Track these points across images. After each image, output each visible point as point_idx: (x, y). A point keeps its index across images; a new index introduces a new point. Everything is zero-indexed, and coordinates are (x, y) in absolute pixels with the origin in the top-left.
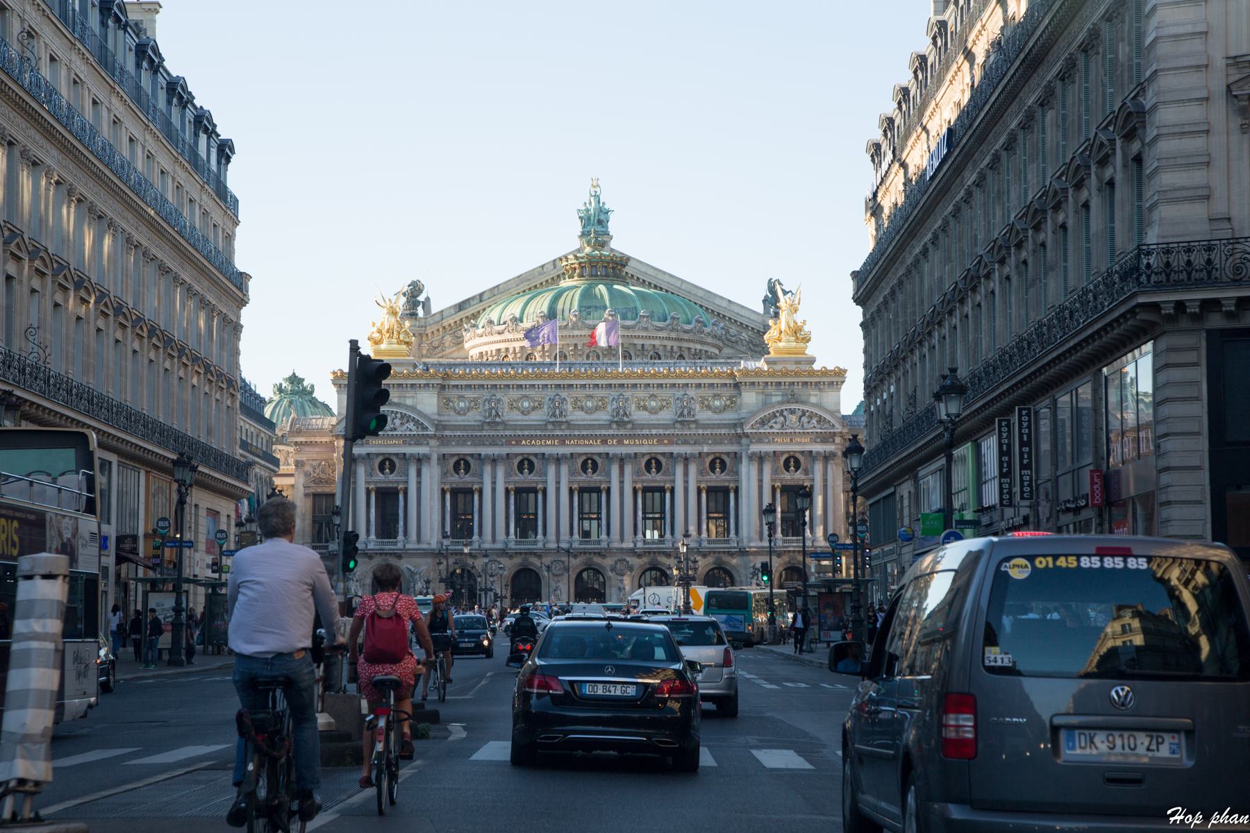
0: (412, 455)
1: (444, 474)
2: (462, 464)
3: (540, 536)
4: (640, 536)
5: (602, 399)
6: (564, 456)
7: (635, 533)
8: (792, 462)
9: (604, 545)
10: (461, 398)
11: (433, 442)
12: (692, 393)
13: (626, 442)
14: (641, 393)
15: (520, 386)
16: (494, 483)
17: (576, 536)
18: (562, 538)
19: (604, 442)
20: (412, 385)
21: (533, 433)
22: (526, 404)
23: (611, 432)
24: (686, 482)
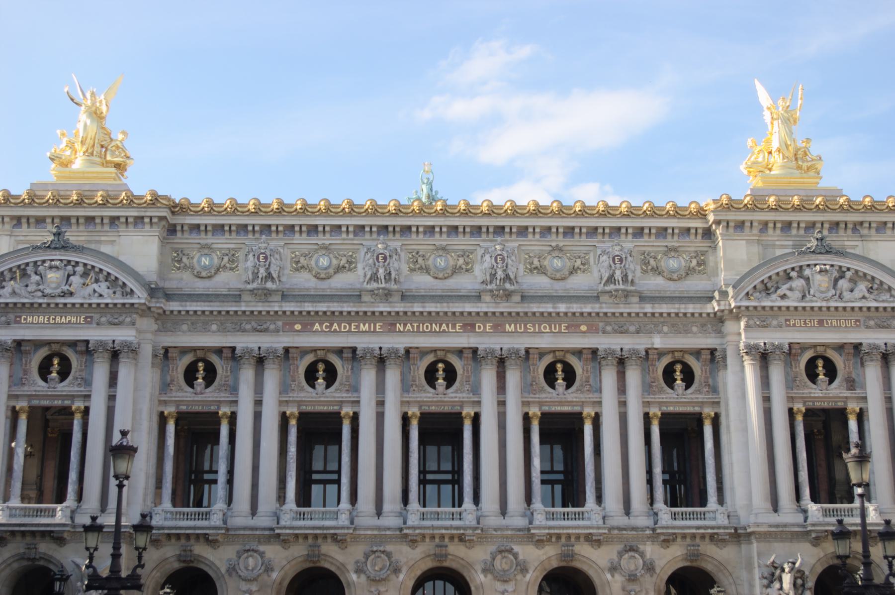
0: (101, 344)
1: (165, 386)
2: (201, 368)
3: (345, 504)
4: (537, 505)
5: (464, 254)
6: (394, 352)
7: (529, 499)
8: (821, 366)
9: (469, 519)
10: (206, 249)
11: (148, 324)
12: (628, 243)
13: (510, 328)
14: (534, 244)
15: (313, 230)
16: (258, 403)
17: (414, 504)
18: (387, 507)
19: (469, 327)
20: (114, 220)
21: (335, 307)
22: (324, 262)
23: (482, 308)
24: (623, 404)
